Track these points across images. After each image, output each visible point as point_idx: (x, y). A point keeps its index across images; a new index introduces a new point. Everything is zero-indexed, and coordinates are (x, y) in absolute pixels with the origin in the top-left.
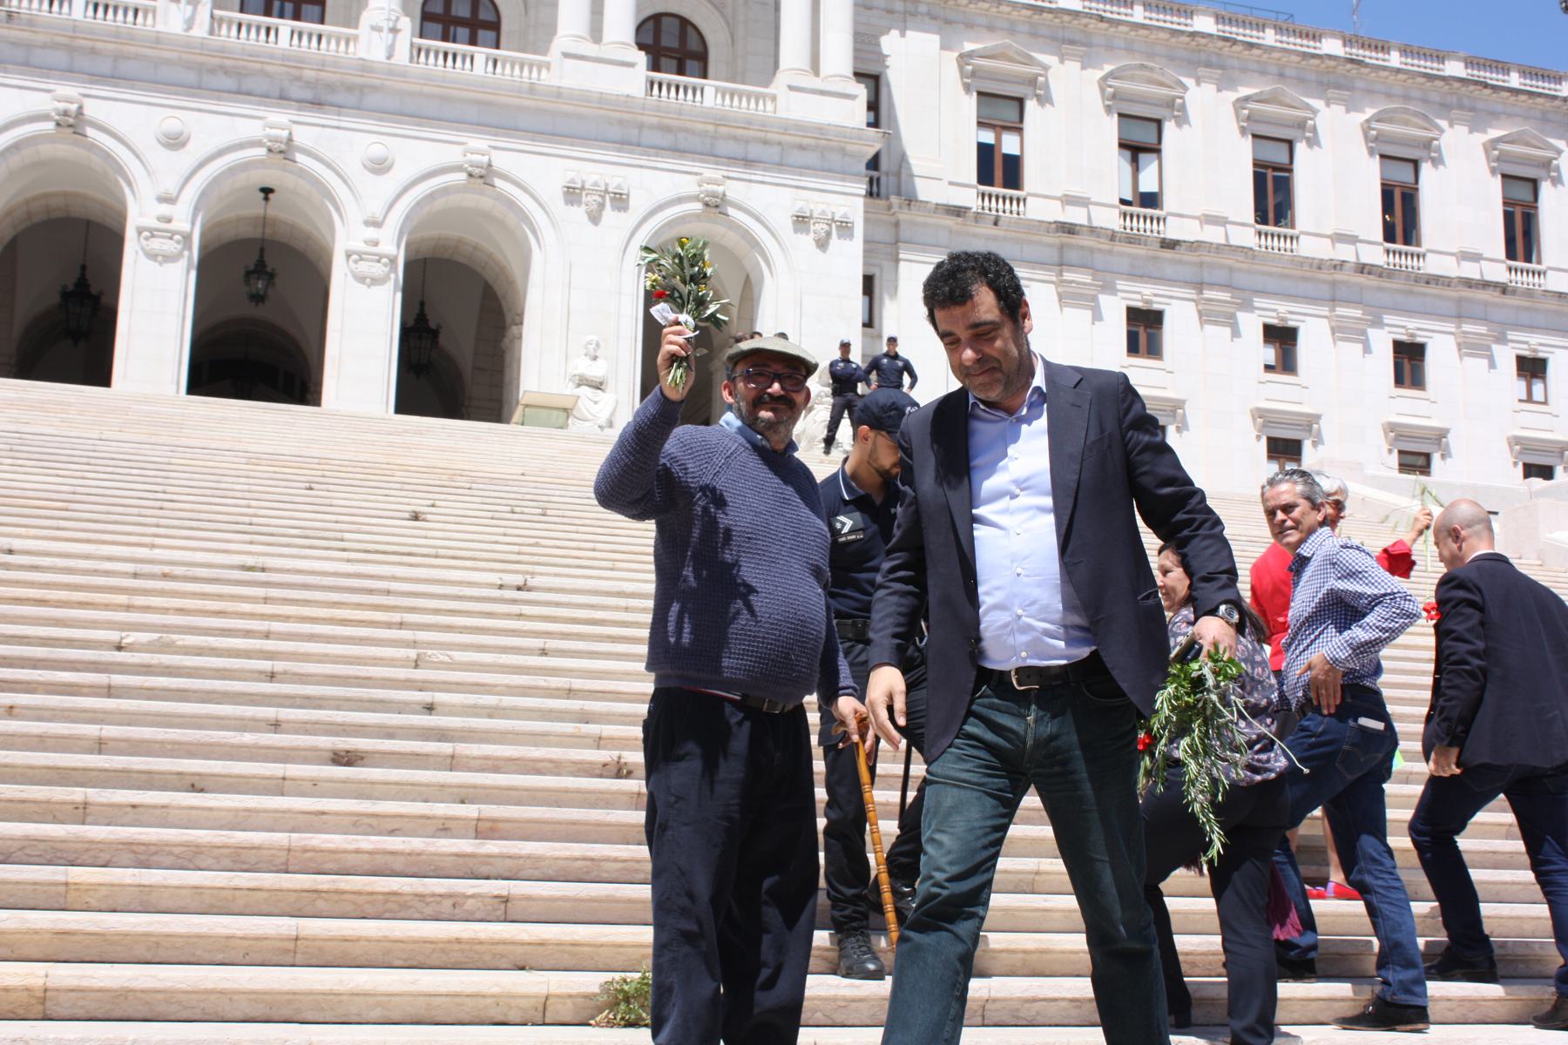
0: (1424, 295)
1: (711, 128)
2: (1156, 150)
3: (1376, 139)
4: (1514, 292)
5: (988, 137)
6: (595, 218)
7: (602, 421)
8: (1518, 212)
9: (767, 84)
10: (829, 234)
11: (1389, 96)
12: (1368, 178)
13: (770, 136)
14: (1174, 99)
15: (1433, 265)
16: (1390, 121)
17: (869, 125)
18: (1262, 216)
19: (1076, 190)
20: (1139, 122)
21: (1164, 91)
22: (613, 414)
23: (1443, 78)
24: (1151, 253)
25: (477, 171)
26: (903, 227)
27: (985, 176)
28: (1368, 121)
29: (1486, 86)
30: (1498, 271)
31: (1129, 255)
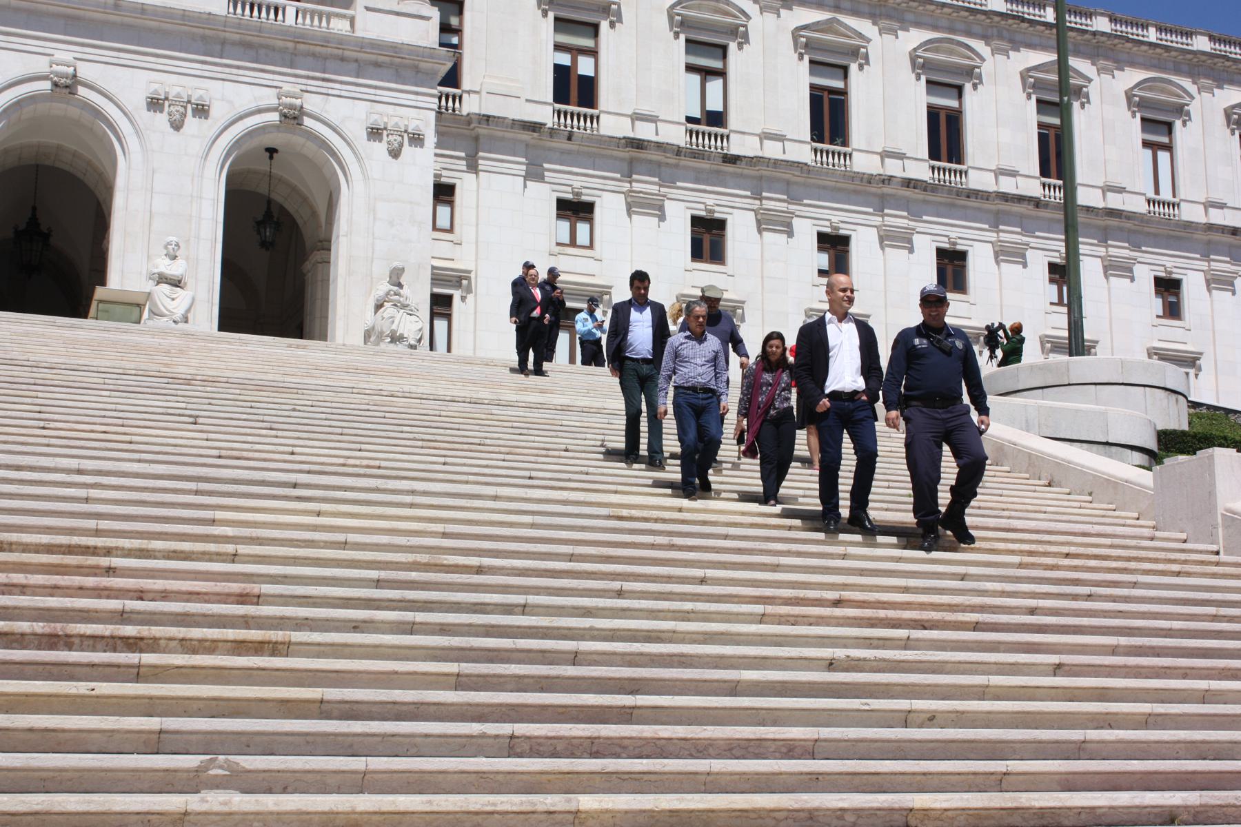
0: (965, 207)
1: (290, 45)
2: (721, 74)
3: (923, 66)
4: (1046, 205)
5: (565, 59)
6: (177, 126)
7: (178, 316)
8: (1052, 134)
9: (347, 8)
10: (401, 145)
11: (935, 28)
12: (915, 100)
13: (347, 53)
14: (738, 26)
15: (978, 180)
16: (936, 50)
17: (441, 45)
18: (817, 133)
19: (645, 109)
20: (707, 48)
21: (730, 20)
22: (188, 310)
23: (985, 13)
24: (715, 167)
25: (63, 81)
26: (482, 140)
27: (561, 94)
28: (915, 50)
29: (1023, 20)
30: (921, 171)
31: (694, 169)
